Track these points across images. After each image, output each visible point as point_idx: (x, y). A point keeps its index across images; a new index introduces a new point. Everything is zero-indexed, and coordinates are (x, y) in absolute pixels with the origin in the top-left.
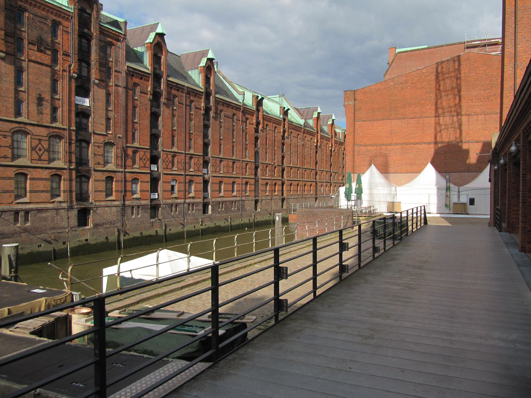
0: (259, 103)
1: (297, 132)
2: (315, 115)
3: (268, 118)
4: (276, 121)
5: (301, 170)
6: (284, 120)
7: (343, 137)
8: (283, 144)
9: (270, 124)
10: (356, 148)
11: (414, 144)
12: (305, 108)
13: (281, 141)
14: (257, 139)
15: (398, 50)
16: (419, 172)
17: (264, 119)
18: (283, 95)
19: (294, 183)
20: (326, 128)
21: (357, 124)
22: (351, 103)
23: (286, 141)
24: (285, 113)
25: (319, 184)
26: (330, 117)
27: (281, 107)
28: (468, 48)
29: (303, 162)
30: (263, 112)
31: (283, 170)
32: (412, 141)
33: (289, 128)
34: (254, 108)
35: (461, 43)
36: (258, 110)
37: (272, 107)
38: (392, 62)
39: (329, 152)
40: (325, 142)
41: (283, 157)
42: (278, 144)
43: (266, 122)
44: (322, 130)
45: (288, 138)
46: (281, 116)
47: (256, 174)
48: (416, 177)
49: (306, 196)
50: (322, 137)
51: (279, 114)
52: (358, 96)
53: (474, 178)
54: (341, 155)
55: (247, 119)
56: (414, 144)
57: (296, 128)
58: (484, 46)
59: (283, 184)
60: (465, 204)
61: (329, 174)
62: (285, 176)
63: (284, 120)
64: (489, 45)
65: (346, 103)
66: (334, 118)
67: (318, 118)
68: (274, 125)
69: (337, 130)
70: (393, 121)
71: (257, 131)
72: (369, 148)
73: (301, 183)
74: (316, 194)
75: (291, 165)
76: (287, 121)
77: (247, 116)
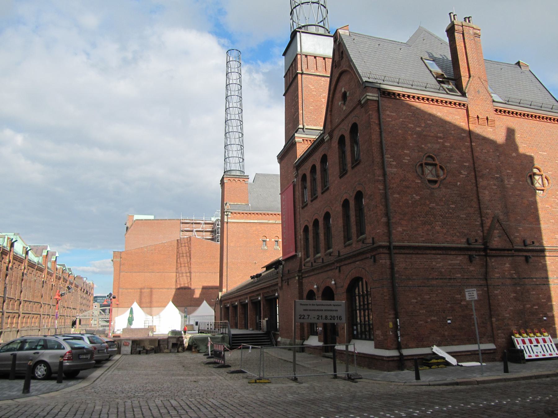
0: (12, 245)
1: (32, 269)
2: (45, 253)
3: (16, 258)
4: (21, 261)
5: (31, 303)
6: (26, 258)
7: (61, 272)
8: (22, 280)
9: (16, 262)
10: (120, 290)
11: (158, 288)
12: (34, 246)
13: (21, 278)
14: (7, 275)
15: (136, 217)
16: (165, 306)
17: (14, 259)
18: (18, 234)
19: (27, 316)
20: (49, 265)
21: (122, 274)
22: (118, 260)
23: (25, 277)
24: (27, 253)
25: (42, 316)
26: (54, 254)
27: (24, 247)
28: (183, 223)
29: (33, 296)
30: (14, 252)
31: (20, 303)
32: (158, 287)
33: (28, 266)
34: (8, 249)
35: (178, 220)
36: (10, 251)
37: (19, 248)
38: (132, 225)
39: (51, 286)
40: (49, 277)
41: (21, 292)
42: (19, 280)
43: (15, 261)
44: (48, 268)
45: (26, 274)
46: (24, 255)
47: (3, 308)
48: (163, 310)
49: (33, 328)
50: (48, 273)
51: (21, 253)
52: (123, 256)
53: (194, 311)
54: (59, 289)
55: (3, 258)
56: (158, 288)
57: (32, 265)
58: (192, 223)
59: (19, 316)
60: (192, 325)
61: (49, 306)
62: (21, 310)
63: (26, 258)
64: (195, 223)
65: (115, 260)
66: (57, 255)
67: (47, 255)
68: (19, 263)
69: (58, 267)
70: (146, 274)
71: (7, 269)
72: (129, 290)
73: (31, 315)
74: (40, 327)
75: (26, 299)
76: (27, 259)
77: (4, 256)
